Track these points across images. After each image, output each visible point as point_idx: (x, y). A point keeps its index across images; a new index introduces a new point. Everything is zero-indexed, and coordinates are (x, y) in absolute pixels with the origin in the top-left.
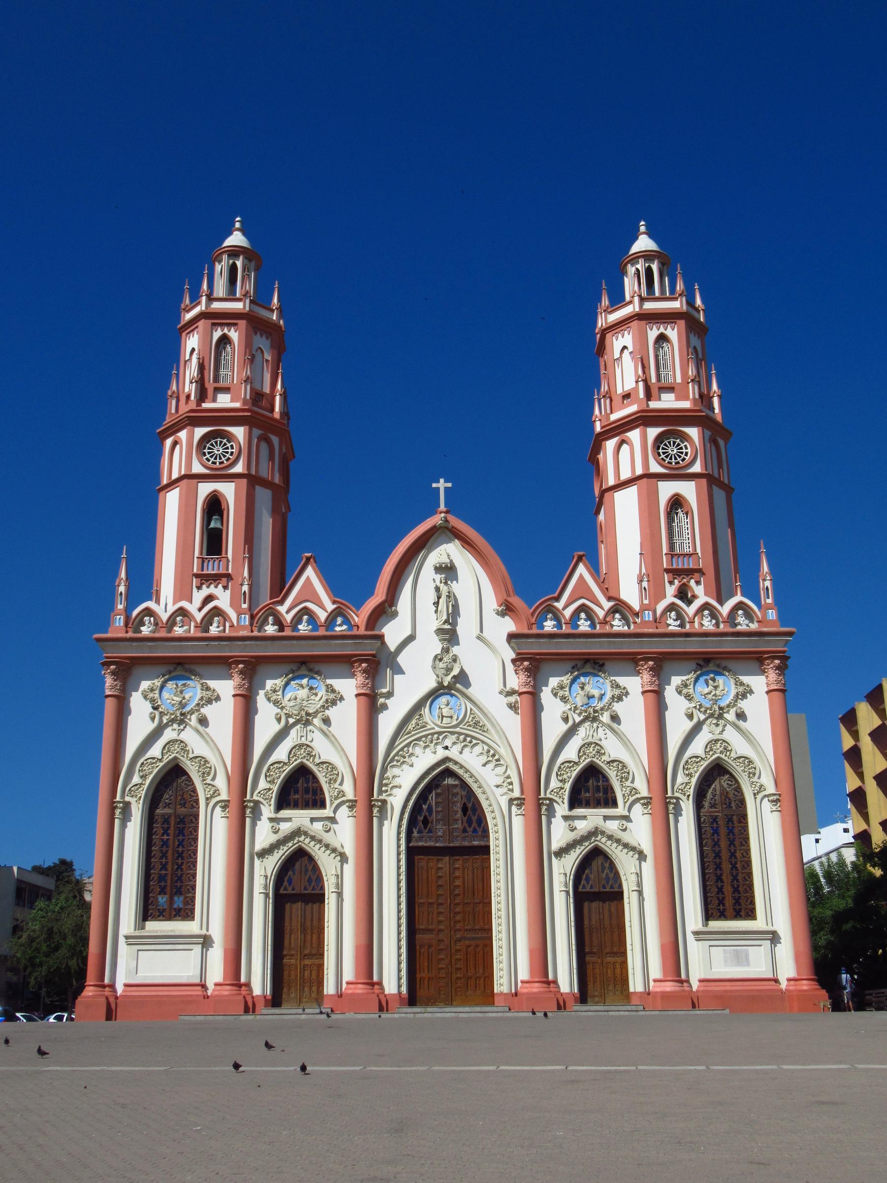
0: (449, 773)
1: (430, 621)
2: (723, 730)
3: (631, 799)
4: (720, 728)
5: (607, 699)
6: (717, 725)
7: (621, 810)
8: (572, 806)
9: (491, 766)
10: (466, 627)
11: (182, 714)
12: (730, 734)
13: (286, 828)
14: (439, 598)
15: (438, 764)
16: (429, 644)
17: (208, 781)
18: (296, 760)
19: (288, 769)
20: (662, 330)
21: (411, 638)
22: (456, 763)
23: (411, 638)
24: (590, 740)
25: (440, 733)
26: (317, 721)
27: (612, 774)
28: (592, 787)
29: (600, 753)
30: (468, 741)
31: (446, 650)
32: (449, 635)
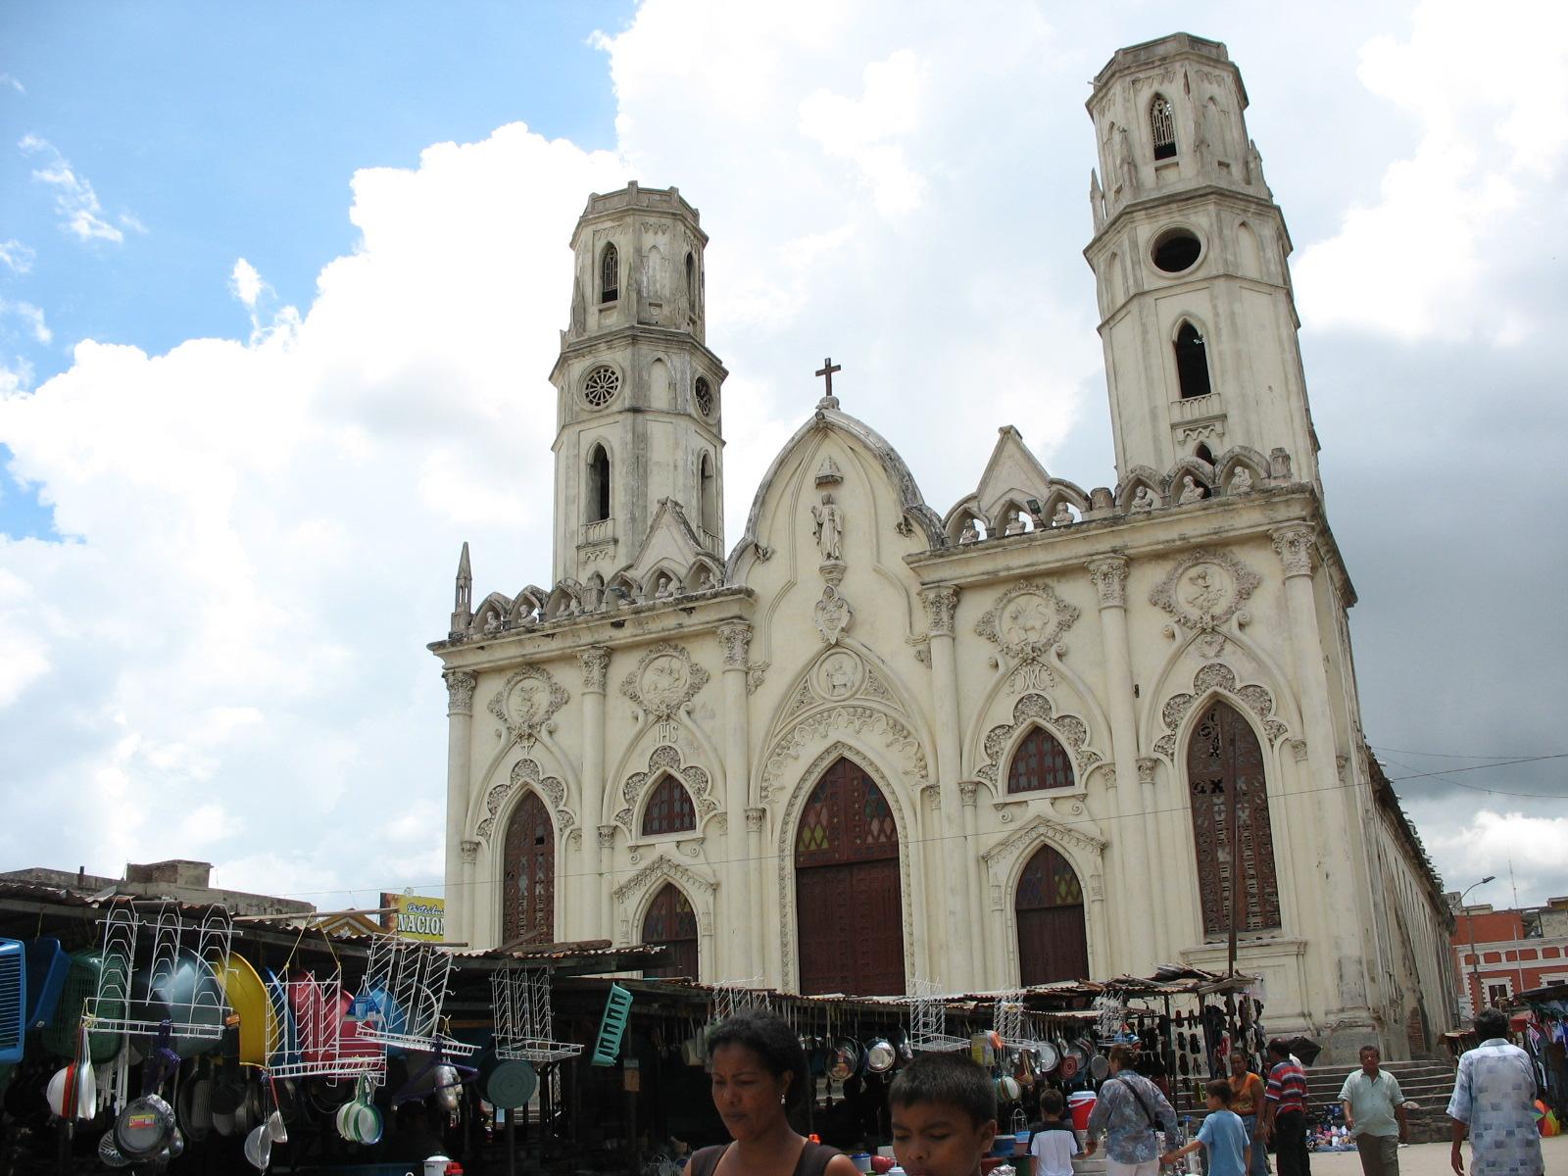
0: (843, 760)
1: (811, 561)
2: (1222, 649)
3: (1090, 769)
4: (1216, 647)
5: (1052, 627)
6: (1210, 644)
7: (1079, 788)
8: (1011, 790)
9: (897, 747)
10: (857, 554)
11: (530, 727)
12: (1231, 658)
13: (649, 858)
14: (820, 525)
15: (827, 751)
16: (812, 587)
17: (561, 808)
18: (658, 769)
19: (650, 781)
20: (1156, 87)
21: (790, 585)
22: (850, 748)
23: (790, 585)
24: (1032, 691)
25: (834, 709)
26: (682, 713)
27: (1062, 737)
28: (1040, 761)
29: (1046, 708)
30: (865, 714)
31: (829, 593)
32: (834, 571)
